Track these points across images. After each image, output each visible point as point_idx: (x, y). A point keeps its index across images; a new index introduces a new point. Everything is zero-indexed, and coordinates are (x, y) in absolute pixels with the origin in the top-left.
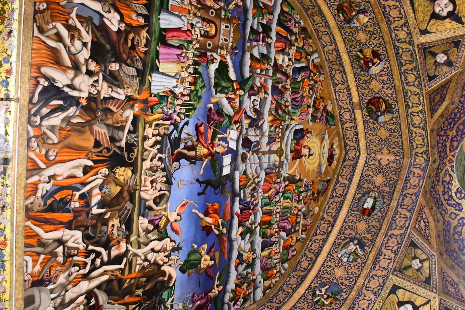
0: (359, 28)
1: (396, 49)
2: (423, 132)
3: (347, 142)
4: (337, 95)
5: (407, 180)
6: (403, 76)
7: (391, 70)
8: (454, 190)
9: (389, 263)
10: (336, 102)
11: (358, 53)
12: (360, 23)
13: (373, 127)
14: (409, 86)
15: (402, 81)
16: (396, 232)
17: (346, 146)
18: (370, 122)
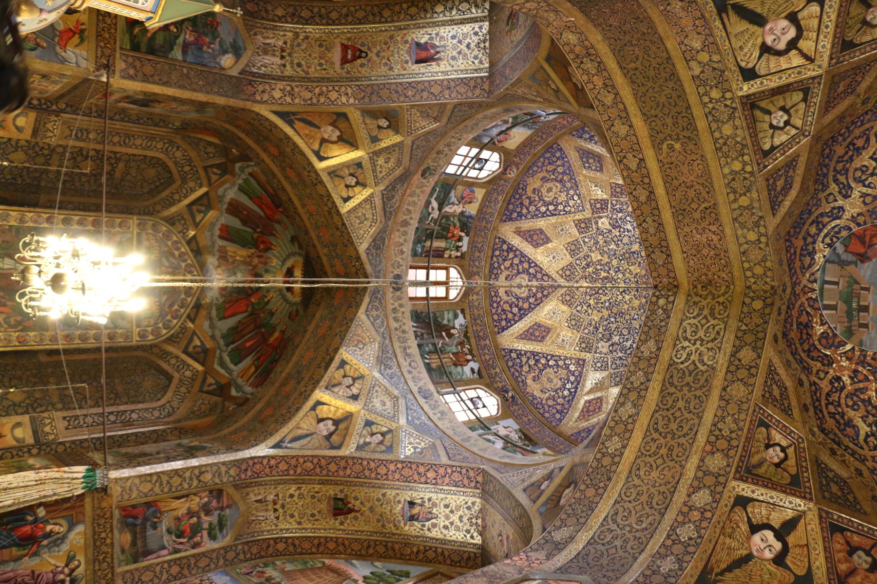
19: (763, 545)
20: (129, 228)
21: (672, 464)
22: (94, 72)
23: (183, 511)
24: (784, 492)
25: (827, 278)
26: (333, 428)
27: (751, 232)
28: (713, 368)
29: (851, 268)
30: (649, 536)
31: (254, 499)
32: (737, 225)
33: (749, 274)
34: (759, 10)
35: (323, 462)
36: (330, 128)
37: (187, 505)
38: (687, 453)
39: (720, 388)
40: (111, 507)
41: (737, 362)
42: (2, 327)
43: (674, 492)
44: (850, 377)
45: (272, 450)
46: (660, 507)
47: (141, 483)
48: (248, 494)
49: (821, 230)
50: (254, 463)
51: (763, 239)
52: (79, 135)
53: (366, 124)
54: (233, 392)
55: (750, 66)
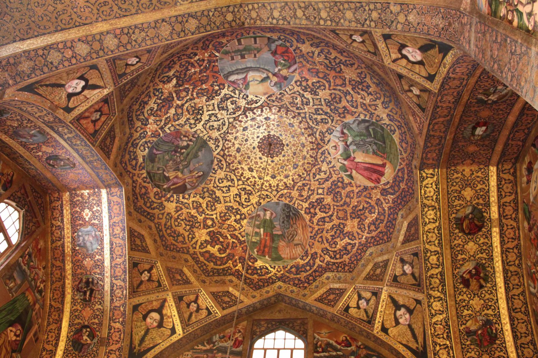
0: (478, 314)
1: (443, 292)
2: (425, 201)
3: (511, 178)
4: (517, 235)
5: (440, 155)
6: (441, 261)
7: (453, 266)
8: (397, 132)
9: (442, 99)
10: (521, 226)
11: (484, 284)
12: (477, 321)
13: (479, 199)
14: (435, 251)
15: (443, 256)
16: (441, 119)
17: (514, 174)
18: (482, 205)
19: (74, 85)
21: (95, 11)
24: (112, 76)
25: (258, 39)
27: (279, 14)
28: (176, 4)
29: (266, 49)
30: (36, 34)
32: (283, 4)
33: (250, 7)
34: (429, 52)
38: (108, 18)
39: (163, 17)
41: (185, 20)
43: (76, 26)
44: (199, 59)
46: (60, 23)
49: (288, 34)
51: (275, 21)
55: (393, 38)
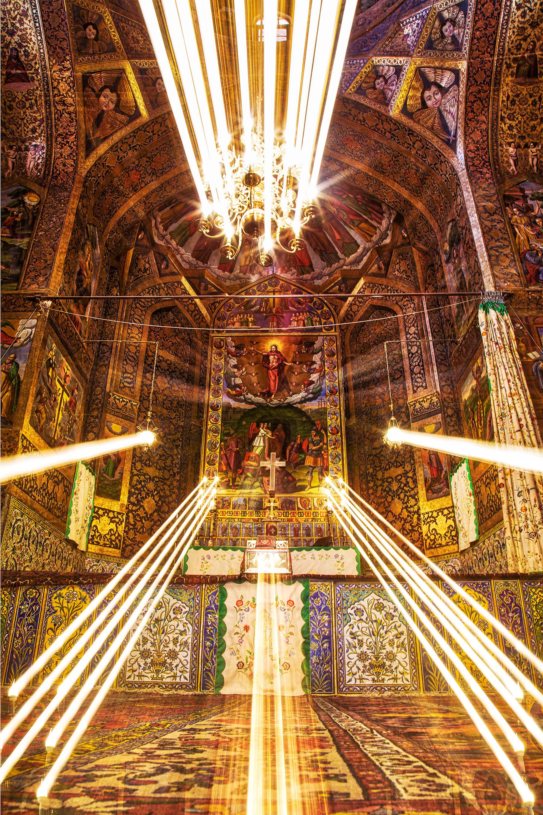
20: (222, 340)
22: (41, 312)
23: (529, 230)
26: (434, 89)
31: (513, 167)
35: (473, 89)
36: (102, 99)
37: (522, 226)
40: (528, 292)
42: (322, 447)
45: (458, 150)
47: (499, 265)
48: (508, 173)
50: (473, 165)
52: (129, 380)
53: (94, 54)
54: (388, 241)
